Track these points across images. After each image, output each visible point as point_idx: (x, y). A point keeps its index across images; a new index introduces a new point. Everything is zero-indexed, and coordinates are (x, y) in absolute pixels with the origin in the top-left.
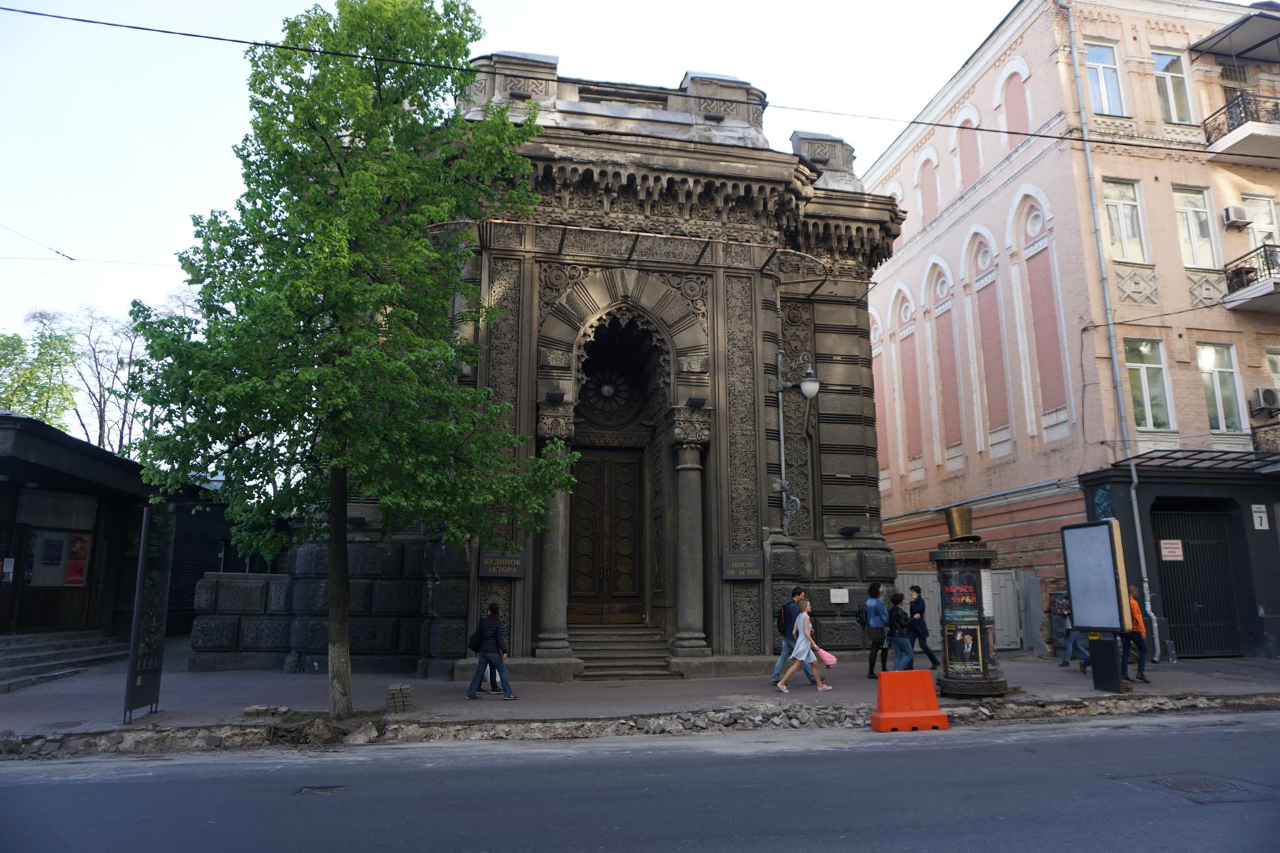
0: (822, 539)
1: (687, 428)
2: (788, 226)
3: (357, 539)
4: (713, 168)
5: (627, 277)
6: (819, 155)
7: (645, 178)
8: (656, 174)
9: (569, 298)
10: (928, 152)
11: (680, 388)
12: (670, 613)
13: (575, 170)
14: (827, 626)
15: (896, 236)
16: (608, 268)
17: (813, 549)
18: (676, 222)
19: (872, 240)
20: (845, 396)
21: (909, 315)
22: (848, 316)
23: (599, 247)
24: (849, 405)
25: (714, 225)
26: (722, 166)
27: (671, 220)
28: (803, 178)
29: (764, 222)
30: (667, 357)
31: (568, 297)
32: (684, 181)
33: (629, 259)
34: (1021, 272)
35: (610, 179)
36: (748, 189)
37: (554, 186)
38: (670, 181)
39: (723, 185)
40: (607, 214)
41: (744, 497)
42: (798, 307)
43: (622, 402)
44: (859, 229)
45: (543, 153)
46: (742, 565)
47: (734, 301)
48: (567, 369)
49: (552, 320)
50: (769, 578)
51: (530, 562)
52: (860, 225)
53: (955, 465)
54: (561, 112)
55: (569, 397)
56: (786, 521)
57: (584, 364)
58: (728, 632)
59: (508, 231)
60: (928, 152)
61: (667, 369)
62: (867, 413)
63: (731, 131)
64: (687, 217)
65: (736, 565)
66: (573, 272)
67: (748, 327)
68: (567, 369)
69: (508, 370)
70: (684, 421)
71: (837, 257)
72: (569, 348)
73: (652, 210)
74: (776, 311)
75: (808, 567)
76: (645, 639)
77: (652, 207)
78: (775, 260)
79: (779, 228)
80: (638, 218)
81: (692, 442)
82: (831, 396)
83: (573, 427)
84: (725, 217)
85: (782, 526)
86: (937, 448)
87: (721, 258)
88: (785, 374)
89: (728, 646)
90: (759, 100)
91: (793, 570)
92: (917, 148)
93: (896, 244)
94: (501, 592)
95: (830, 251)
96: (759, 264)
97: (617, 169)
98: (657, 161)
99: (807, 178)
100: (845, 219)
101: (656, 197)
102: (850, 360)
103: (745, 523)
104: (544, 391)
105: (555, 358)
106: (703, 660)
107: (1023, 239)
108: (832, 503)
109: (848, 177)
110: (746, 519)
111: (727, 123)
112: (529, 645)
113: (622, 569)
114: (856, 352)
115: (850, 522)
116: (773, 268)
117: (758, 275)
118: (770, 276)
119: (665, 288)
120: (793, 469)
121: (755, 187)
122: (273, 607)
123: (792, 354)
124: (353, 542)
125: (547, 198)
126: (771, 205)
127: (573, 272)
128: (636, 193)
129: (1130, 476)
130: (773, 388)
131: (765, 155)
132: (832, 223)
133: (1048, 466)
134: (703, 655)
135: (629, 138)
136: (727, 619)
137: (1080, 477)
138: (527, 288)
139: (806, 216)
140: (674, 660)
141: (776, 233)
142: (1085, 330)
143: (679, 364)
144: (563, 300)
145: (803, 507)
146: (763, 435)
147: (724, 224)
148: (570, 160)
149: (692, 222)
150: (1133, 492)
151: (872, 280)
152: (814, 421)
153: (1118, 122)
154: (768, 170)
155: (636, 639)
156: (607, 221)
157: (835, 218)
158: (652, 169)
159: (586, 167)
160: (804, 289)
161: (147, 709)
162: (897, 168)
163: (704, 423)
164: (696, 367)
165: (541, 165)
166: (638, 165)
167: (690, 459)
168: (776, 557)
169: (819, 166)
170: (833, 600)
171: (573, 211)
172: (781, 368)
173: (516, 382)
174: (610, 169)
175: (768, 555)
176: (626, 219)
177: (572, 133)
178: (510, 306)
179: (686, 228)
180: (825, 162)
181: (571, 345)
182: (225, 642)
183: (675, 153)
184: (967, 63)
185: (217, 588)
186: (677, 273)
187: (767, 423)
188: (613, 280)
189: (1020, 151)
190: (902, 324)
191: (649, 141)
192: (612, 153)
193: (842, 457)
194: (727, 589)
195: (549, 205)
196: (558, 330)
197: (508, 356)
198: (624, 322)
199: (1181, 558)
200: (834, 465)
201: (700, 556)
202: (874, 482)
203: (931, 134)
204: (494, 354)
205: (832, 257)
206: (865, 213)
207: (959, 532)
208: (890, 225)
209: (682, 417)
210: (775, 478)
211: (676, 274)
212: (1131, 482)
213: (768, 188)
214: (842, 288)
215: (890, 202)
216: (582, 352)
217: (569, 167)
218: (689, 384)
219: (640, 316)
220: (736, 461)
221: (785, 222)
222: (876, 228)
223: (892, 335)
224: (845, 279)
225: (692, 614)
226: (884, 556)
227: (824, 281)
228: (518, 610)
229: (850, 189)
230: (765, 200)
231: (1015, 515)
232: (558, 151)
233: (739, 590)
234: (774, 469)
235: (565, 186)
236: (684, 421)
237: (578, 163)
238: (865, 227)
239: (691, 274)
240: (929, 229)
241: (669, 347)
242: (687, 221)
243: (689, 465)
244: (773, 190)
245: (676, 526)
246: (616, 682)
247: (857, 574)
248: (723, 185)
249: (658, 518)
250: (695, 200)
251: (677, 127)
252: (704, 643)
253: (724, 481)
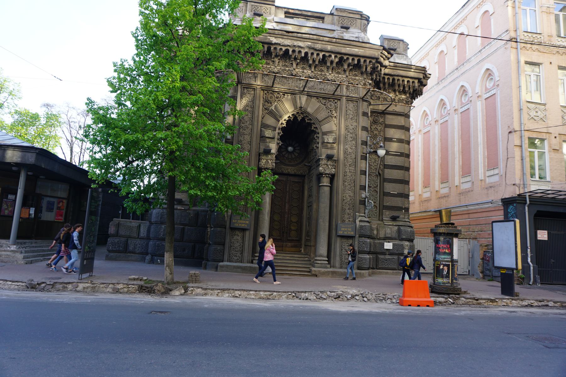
0: (382, 220)
1: (325, 167)
2: (376, 79)
3: (179, 208)
4: (344, 50)
5: (302, 99)
6: (392, 46)
7: (312, 54)
8: (317, 52)
9: (276, 107)
10: (442, 47)
11: (323, 150)
12: (313, 248)
13: (281, 49)
14: (382, 259)
15: (425, 85)
16: (293, 94)
17: (378, 224)
18: (325, 75)
19: (414, 87)
20: (397, 157)
21: (428, 122)
22: (400, 121)
23: (290, 85)
24: (398, 161)
25: (342, 76)
27: (323, 73)
28: (384, 57)
29: (365, 76)
30: (318, 135)
31: (275, 106)
32: (330, 56)
33: (303, 91)
34: (482, 104)
35: (297, 54)
36: (359, 61)
37: (271, 56)
38: (324, 56)
39: (348, 58)
40: (294, 69)
41: (348, 200)
42: (378, 116)
43: (297, 155)
44: (408, 81)
45: (267, 41)
46: (346, 229)
47: (349, 111)
48: (273, 138)
49: (267, 116)
50: (357, 236)
51: (253, 222)
52: (409, 79)
53: (444, 191)
54: (276, 22)
55: (273, 151)
56: (367, 211)
57: (280, 137)
58: (338, 258)
59: (250, 75)
60: (442, 47)
61: (318, 140)
62: (406, 165)
63: (353, 34)
64: (331, 72)
65: (343, 229)
66: (278, 95)
67: (355, 124)
68: (273, 138)
69: (247, 138)
70: (324, 164)
71: (397, 94)
72: (274, 129)
73: (315, 69)
74: (368, 117)
75: (375, 232)
76: (301, 259)
77: (315, 67)
78: (369, 94)
79: (372, 79)
80: (308, 72)
81: (327, 174)
82: (391, 157)
83: (274, 164)
84: (347, 73)
85: (365, 213)
86: (437, 183)
87: (345, 92)
88: (370, 146)
89: (337, 264)
90: (367, 19)
91: (368, 233)
92: (437, 45)
93: (425, 89)
94: (240, 234)
95: (395, 91)
96: (362, 95)
97: (300, 49)
98: (319, 46)
99: (386, 57)
100: (402, 76)
101: (317, 63)
102: (400, 141)
103: (348, 211)
104: (262, 148)
105: (268, 133)
106: (326, 270)
107: (484, 89)
108: (388, 204)
109: (405, 57)
110: (349, 209)
111: (351, 30)
112: (251, 258)
113: (293, 228)
114: (403, 137)
115: (395, 214)
116: (368, 97)
117: (361, 100)
118: (366, 101)
119: (319, 104)
120: (371, 188)
121: (362, 60)
122: (142, 235)
123: (374, 137)
124: (177, 209)
125: (268, 61)
126: (369, 69)
127: (278, 95)
128: (308, 61)
129: (526, 201)
130: (365, 151)
131: (367, 45)
132: (396, 78)
133: (488, 194)
134: (326, 268)
135: (306, 35)
136: (338, 253)
137: (502, 199)
138: (257, 102)
139: (385, 74)
140: (313, 269)
141: (370, 82)
142: (510, 132)
143: (323, 139)
144: (273, 108)
145: (374, 206)
146: (359, 172)
147: (347, 76)
148: (279, 44)
149: (332, 75)
150: (527, 208)
151: (413, 105)
152: (382, 167)
153: (534, 35)
154: (368, 53)
155: (297, 259)
156: (294, 73)
157: (398, 76)
158: (316, 50)
159: (286, 48)
160: (382, 108)
161: (88, 274)
162: (427, 54)
163: (333, 165)
165: (266, 46)
166: (310, 48)
167: (325, 181)
168: (361, 227)
169: (392, 52)
170: (385, 248)
171: (279, 68)
172: (369, 143)
173: (250, 143)
174: (297, 49)
175: (358, 226)
176: (303, 72)
177: (280, 32)
178: (250, 109)
179: (330, 77)
180: (394, 50)
181: (275, 128)
182: (121, 249)
183: (326, 43)
184: (464, 6)
185: (118, 225)
186: (325, 98)
187: (361, 167)
188: (295, 99)
189: (486, 48)
190: (424, 126)
191: (315, 37)
192: (298, 42)
193: (394, 184)
194: (339, 240)
195: (268, 64)
196: (270, 121)
197: (247, 131)
198: (299, 119)
199: (546, 239)
200: (390, 188)
201: (327, 224)
202: (407, 196)
203: (445, 38)
204: (241, 130)
205: (395, 93)
206: (412, 74)
207: (445, 220)
208: (423, 80)
209: (323, 163)
210: (363, 192)
211: (324, 98)
212: (526, 203)
213: (368, 60)
214: (399, 108)
215: (424, 69)
216: (280, 131)
217: (279, 47)
218: (327, 148)
219: (307, 116)
220: (346, 184)
221: (374, 77)
222: (416, 81)
223: (420, 131)
224: (400, 104)
225: (323, 249)
226: (409, 229)
227: (391, 104)
228: (247, 243)
229: (406, 63)
230: (366, 66)
231: (470, 215)
232: (274, 40)
233: (344, 240)
234: (363, 188)
235: (276, 56)
236: (324, 164)
237: (283, 46)
238: (411, 80)
239: (331, 98)
240: (440, 83)
241: (319, 131)
242: (330, 74)
243: (325, 184)
244: (370, 62)
245: (318, 211)
246: (287, 276)
247: (397, 236)
248: (348, 58)
249: (310, 206)
250: (334, 65)
251: (328, 31)
252: (327, 262)
253: (340, 192)
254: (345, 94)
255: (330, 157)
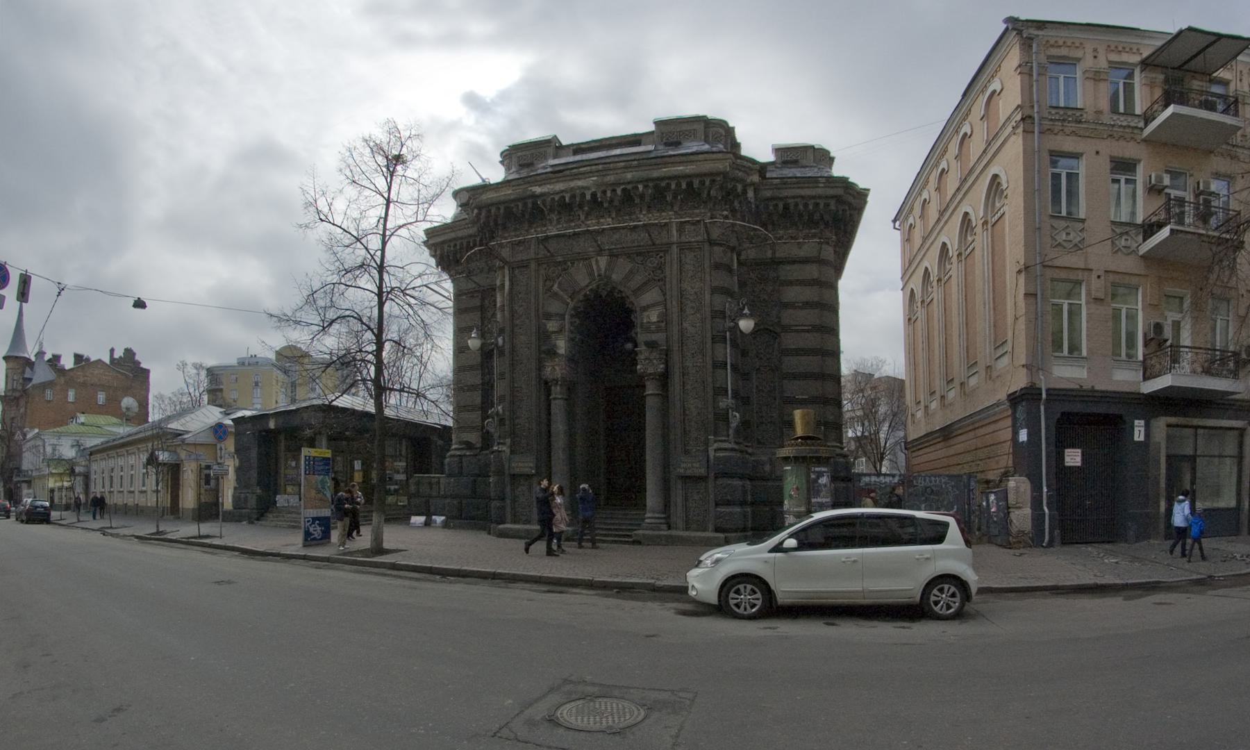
1: (648, 364)
26: (665, 171)
36: (690, 185)
39: (669, 185)
56: (731, 431)
72: (562, 317)
84: (676, 208)
105: (552, 326)
117: (706, 246)
119: (630, 266)
146: (709, 366)
153: (1070, 113)
163: (660, 359)
164: (654, 319)
172: (728, 313)
175: (711, 457)
196: (555, 307)
198: (604, 294)
211: (639, 254)
219: (614, 288)
234: (721, 391)
254: (675, 239)
255: (652, 345)
